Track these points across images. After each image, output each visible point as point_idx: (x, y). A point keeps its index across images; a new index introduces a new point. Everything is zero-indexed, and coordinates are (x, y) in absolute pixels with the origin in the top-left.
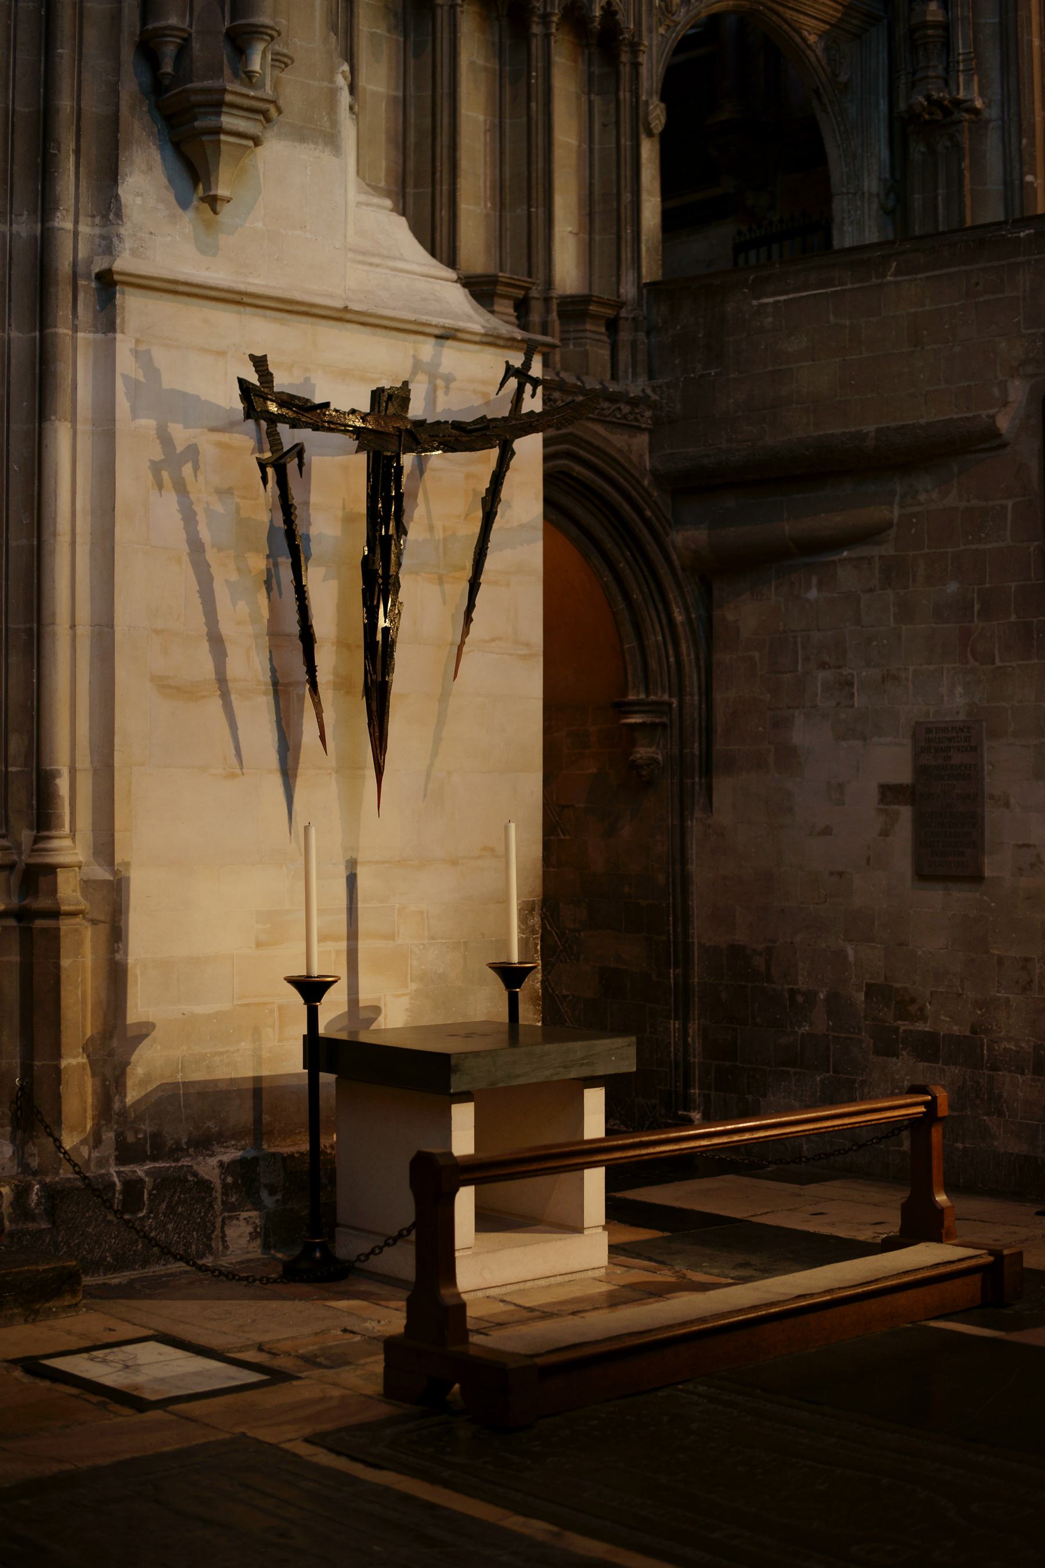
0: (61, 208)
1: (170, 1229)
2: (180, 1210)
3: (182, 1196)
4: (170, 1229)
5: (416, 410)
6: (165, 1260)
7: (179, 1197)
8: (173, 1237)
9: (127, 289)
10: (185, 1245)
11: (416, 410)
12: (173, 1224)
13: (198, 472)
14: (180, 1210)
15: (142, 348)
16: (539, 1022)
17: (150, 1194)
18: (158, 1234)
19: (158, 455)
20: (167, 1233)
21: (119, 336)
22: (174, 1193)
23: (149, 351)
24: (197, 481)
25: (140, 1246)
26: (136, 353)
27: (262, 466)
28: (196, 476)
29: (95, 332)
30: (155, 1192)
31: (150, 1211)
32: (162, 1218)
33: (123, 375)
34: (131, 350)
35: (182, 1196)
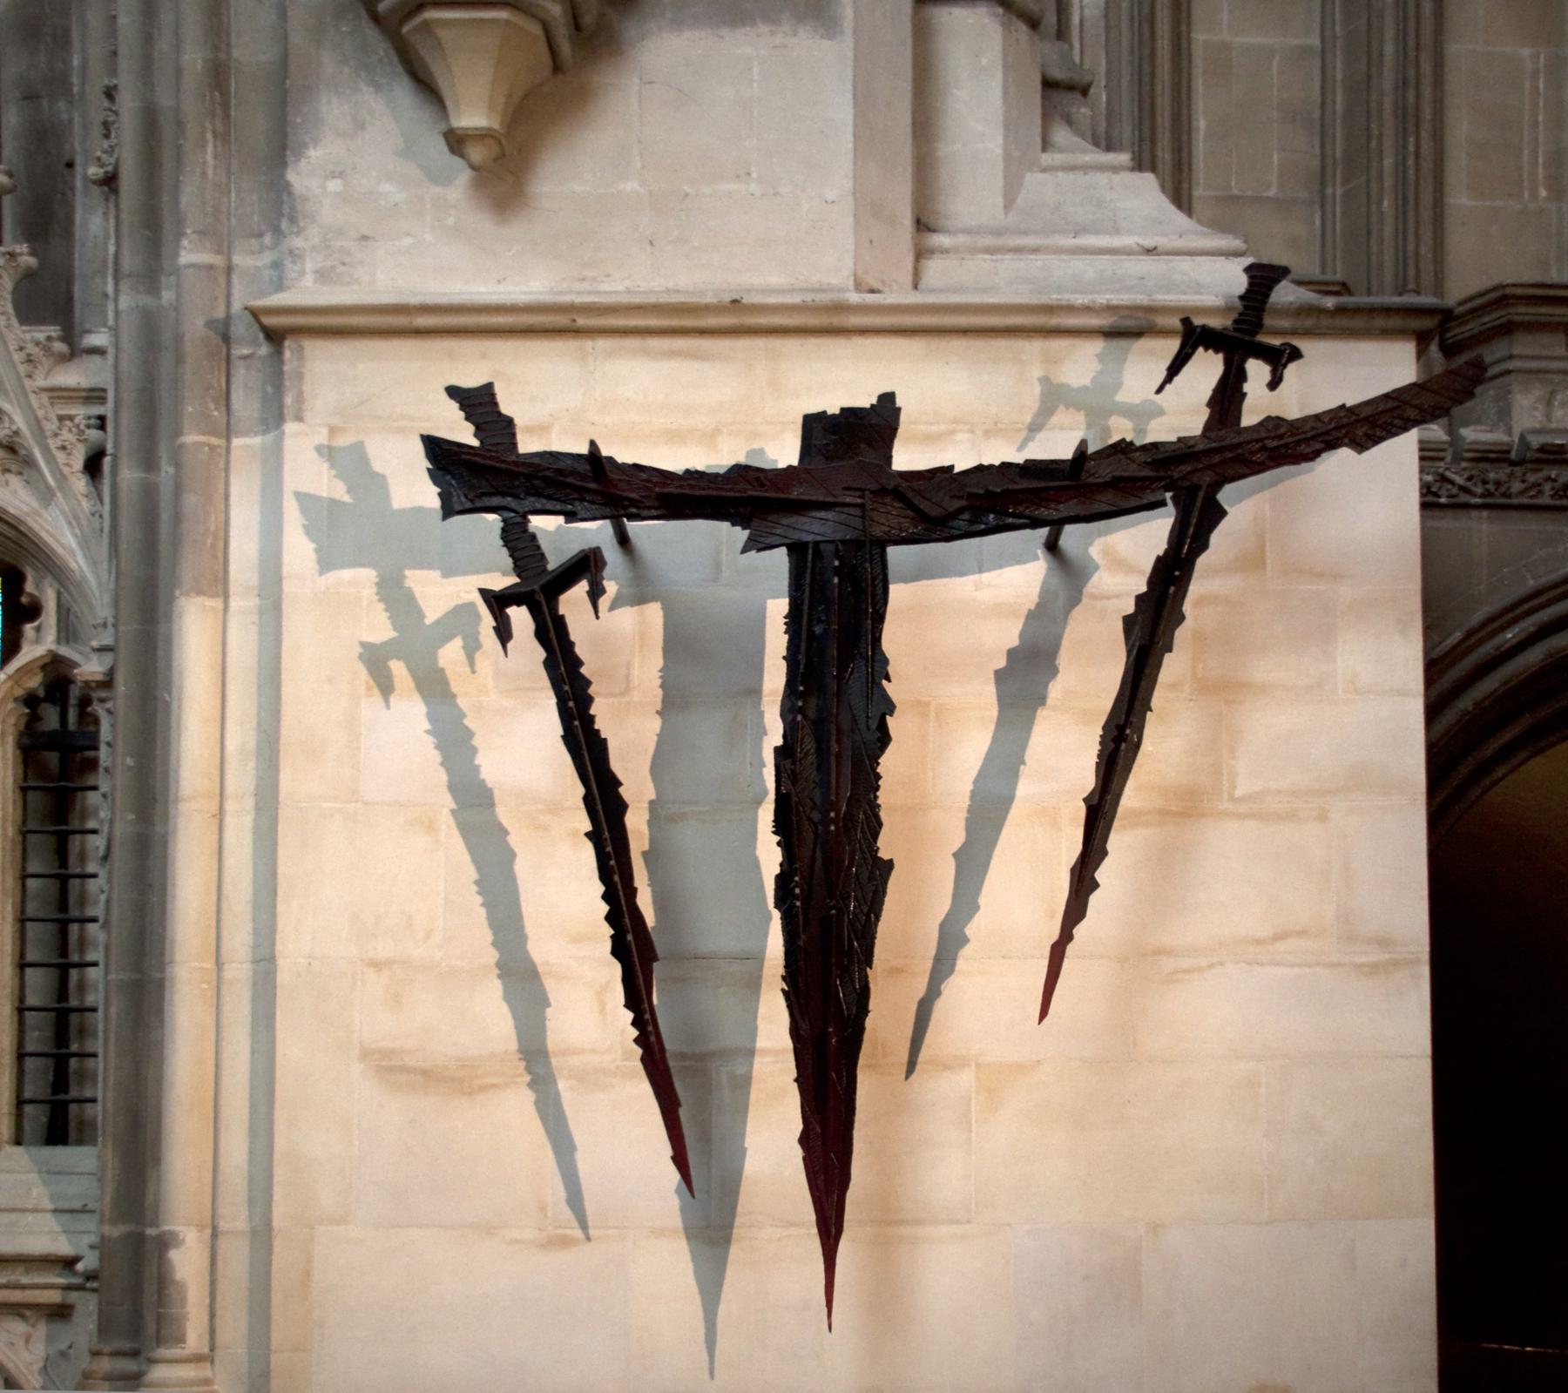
0: (189, 231)
5: (906, 457)
9: (313, 347)
11: (906, 457)
13: (478, 656)
15: (343, 441)
19: (380, 630)
21: (290, 427)
23: (359, 447)
24: (474, 672)
26: (328, 453)
27: (498, 602)
28: (472, 664)
29: (264, 432)
33: (299, 496)
34: (319, 449)
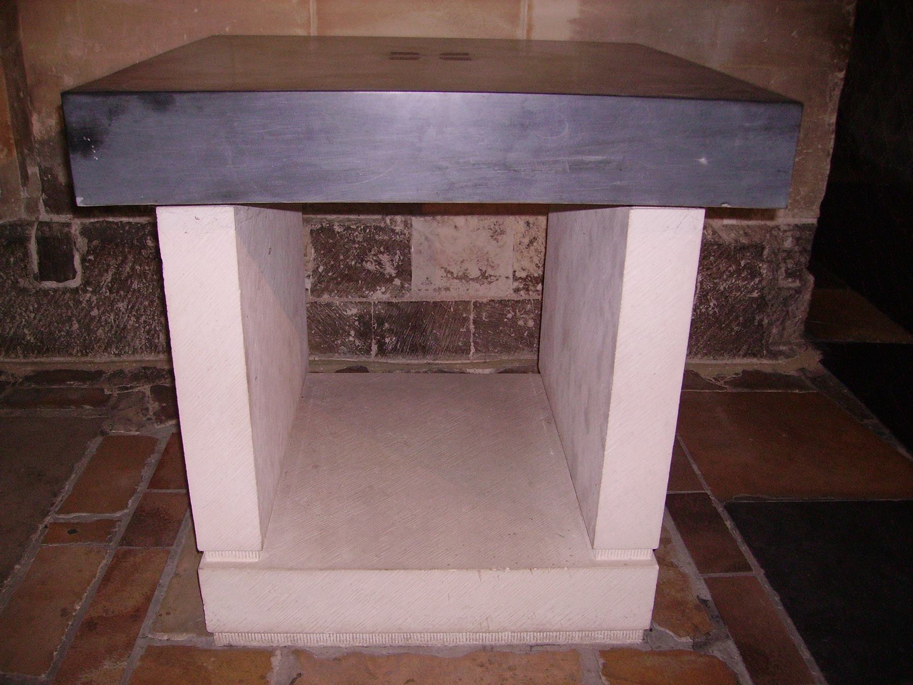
1: (123, 310)
2: (135, 286)
3: (138, 267)
4: (123, 310)
6: (117, 348)
7: (133, 268)
8: (128, 321)
10: (148, 332)
12: (125, 303)
14: (135, 286)
16: (840, 70)
17: (83, 260)
18: (103, 313)
20: (117, 314)
22: (124, 261)
25: (76, 326)
30: (91, 257)
31: (86, 283)
32: (108, 294)
35: (138, 267)
